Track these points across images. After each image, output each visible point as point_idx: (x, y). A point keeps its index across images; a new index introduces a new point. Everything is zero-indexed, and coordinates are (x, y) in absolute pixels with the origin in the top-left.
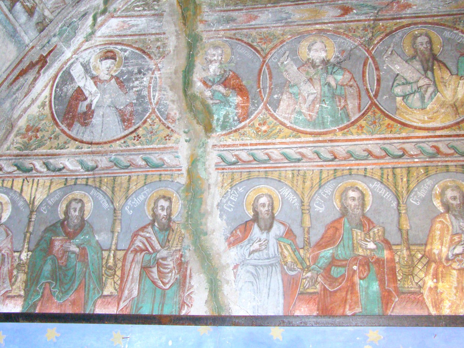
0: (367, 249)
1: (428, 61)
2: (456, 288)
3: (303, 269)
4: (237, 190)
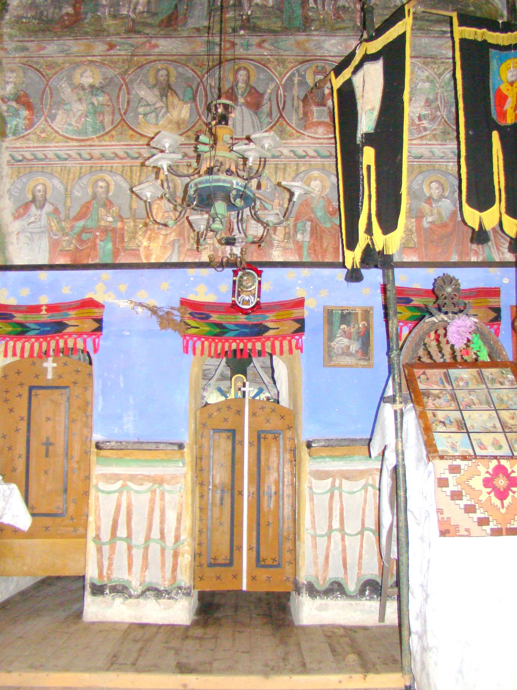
0: (107, 221)
1: (164, 89)
2: (161, 247)
3: (63, 235)
4: (21, 180)
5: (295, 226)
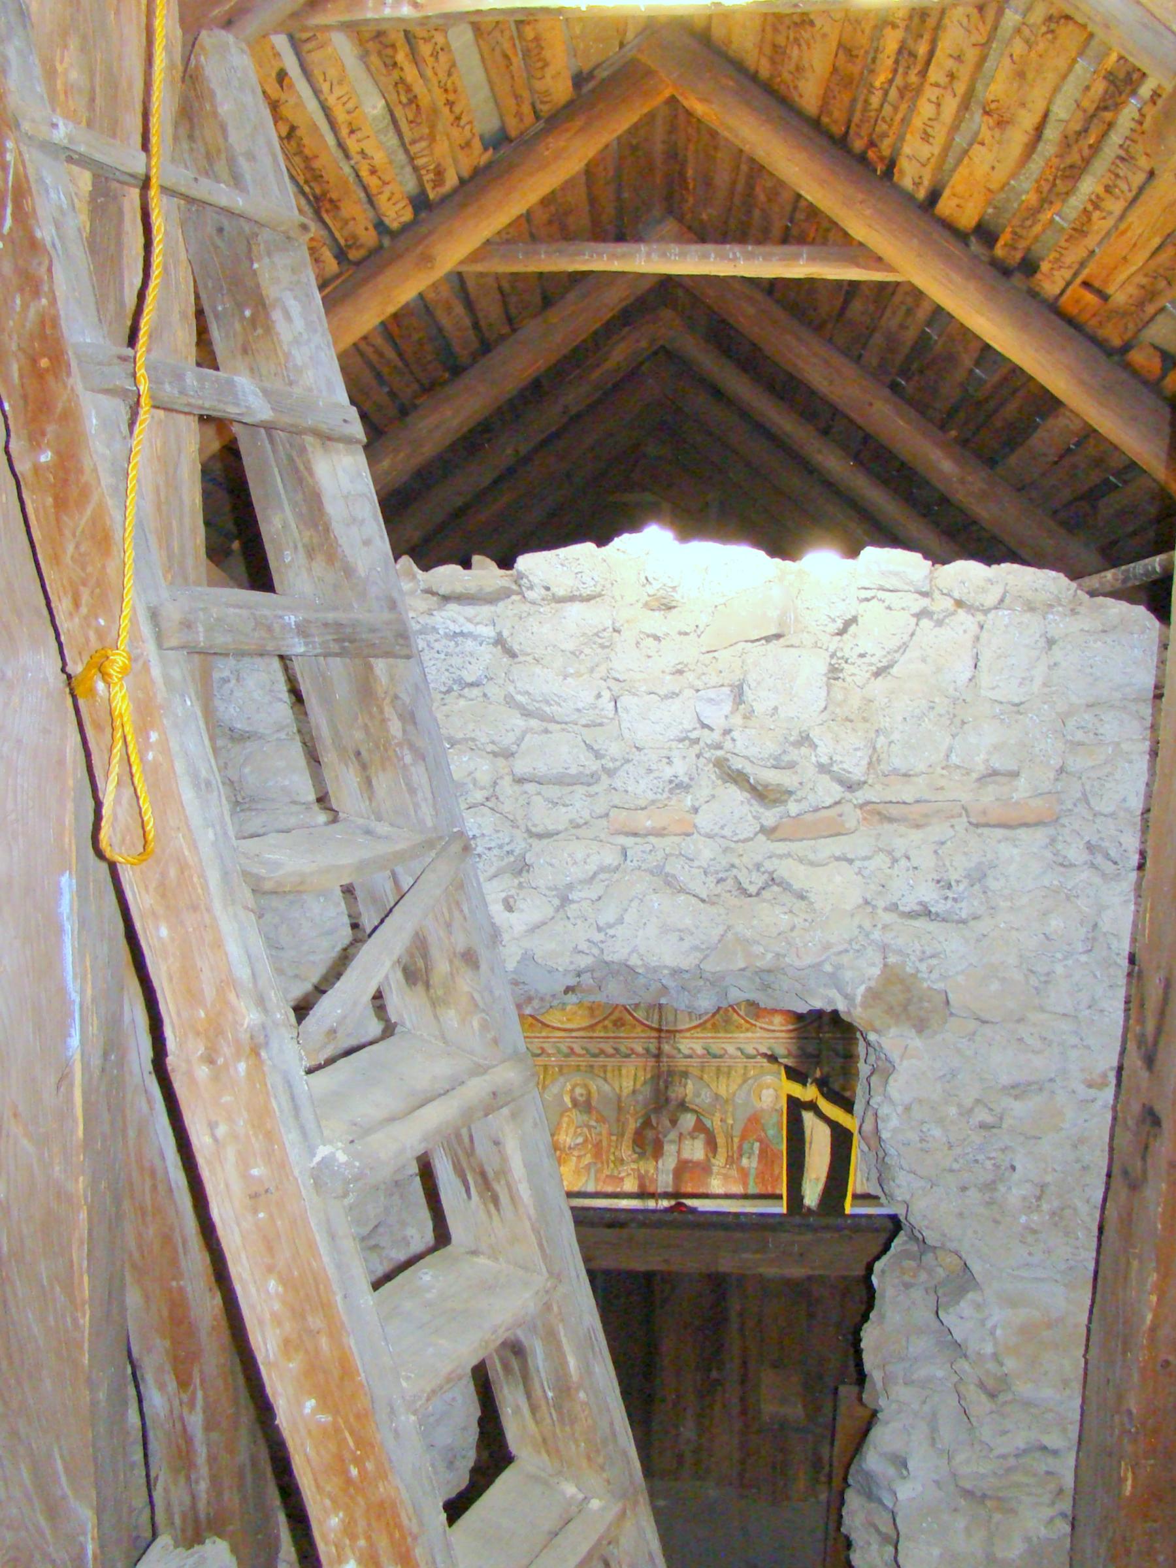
5: (740, 1148)
